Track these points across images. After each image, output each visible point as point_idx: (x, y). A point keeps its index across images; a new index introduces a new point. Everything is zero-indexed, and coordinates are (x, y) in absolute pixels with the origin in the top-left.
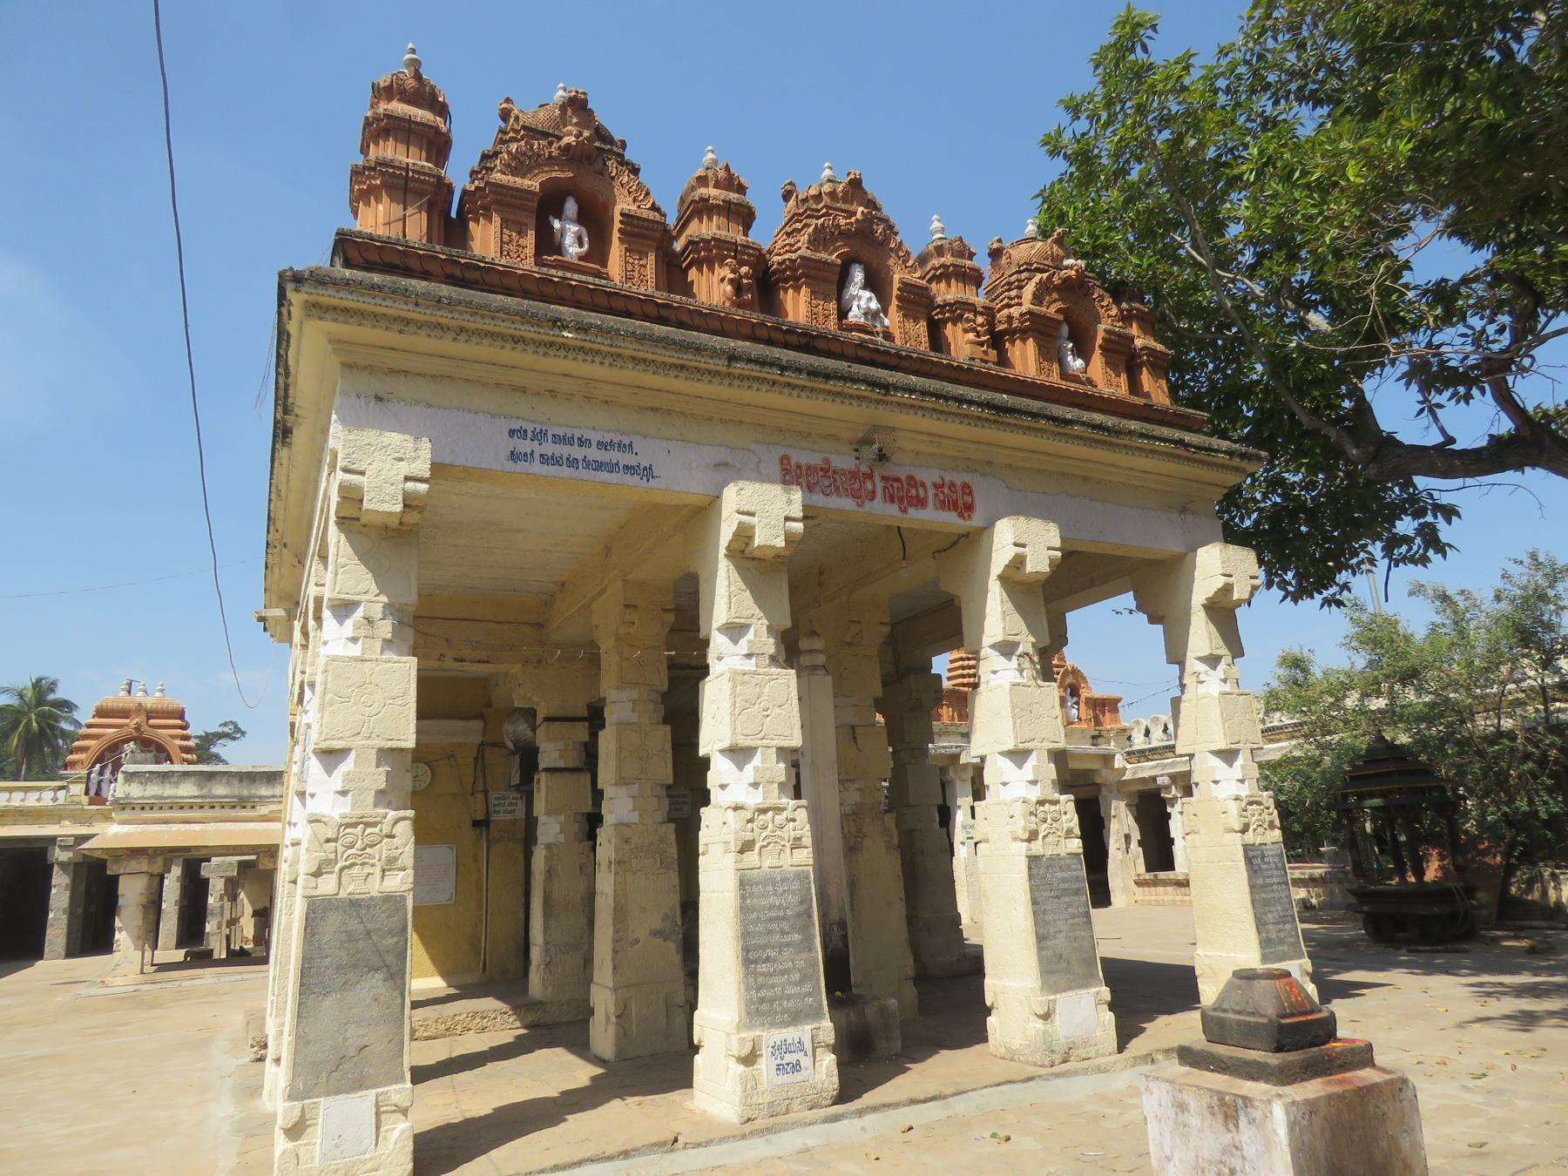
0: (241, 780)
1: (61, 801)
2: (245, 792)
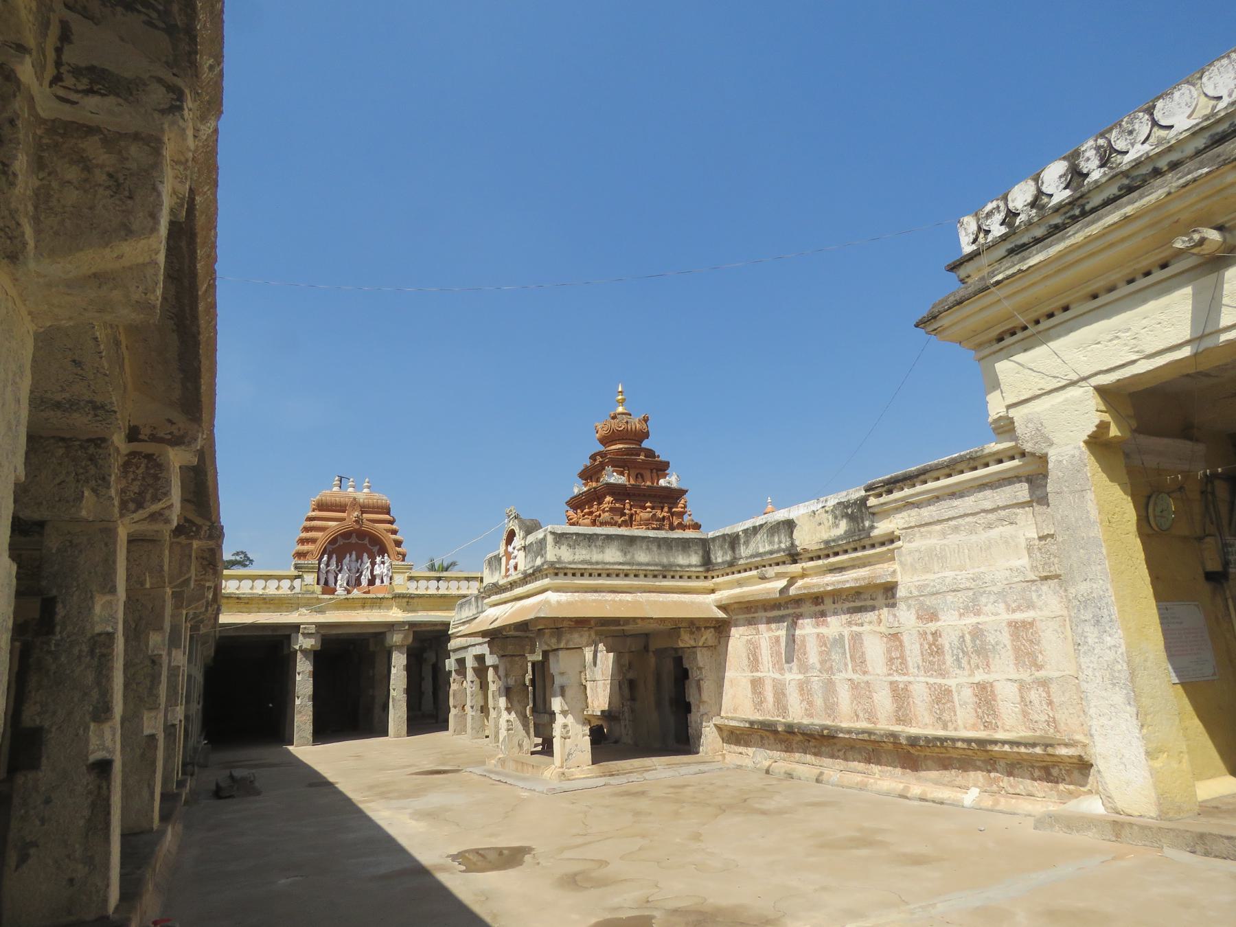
0: (659, 547)
1: (297, 590)
2: (665, 561)
